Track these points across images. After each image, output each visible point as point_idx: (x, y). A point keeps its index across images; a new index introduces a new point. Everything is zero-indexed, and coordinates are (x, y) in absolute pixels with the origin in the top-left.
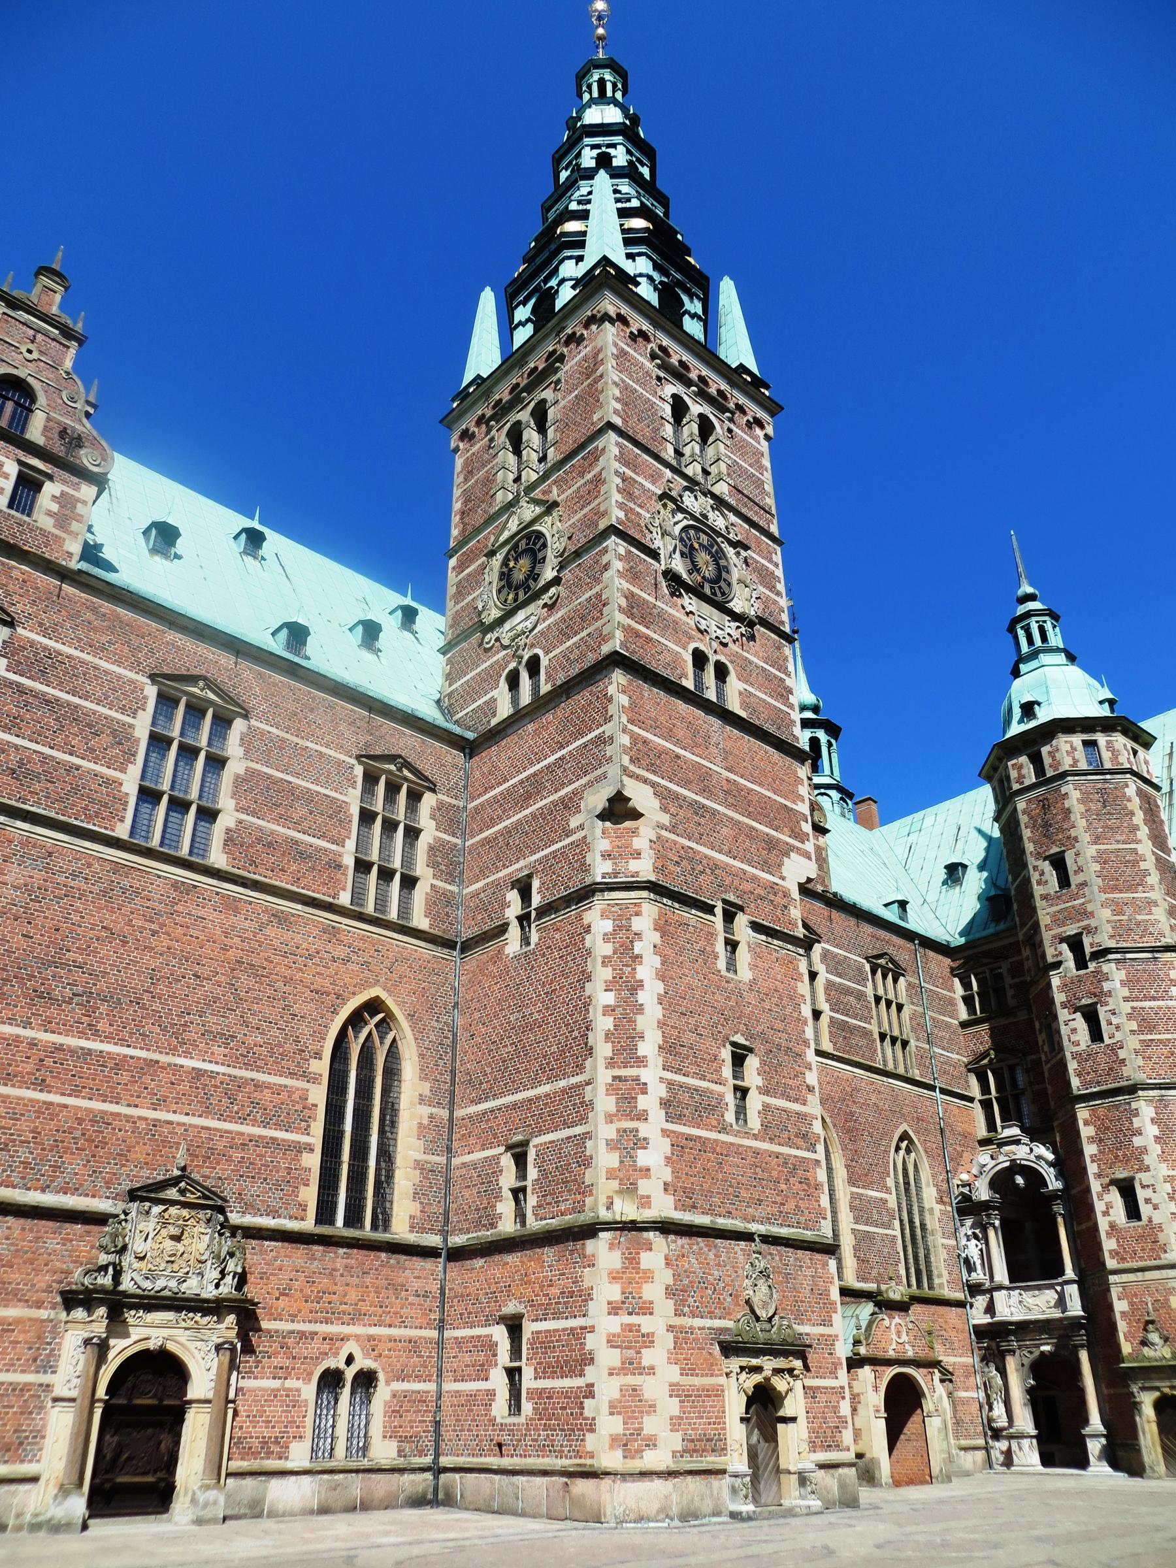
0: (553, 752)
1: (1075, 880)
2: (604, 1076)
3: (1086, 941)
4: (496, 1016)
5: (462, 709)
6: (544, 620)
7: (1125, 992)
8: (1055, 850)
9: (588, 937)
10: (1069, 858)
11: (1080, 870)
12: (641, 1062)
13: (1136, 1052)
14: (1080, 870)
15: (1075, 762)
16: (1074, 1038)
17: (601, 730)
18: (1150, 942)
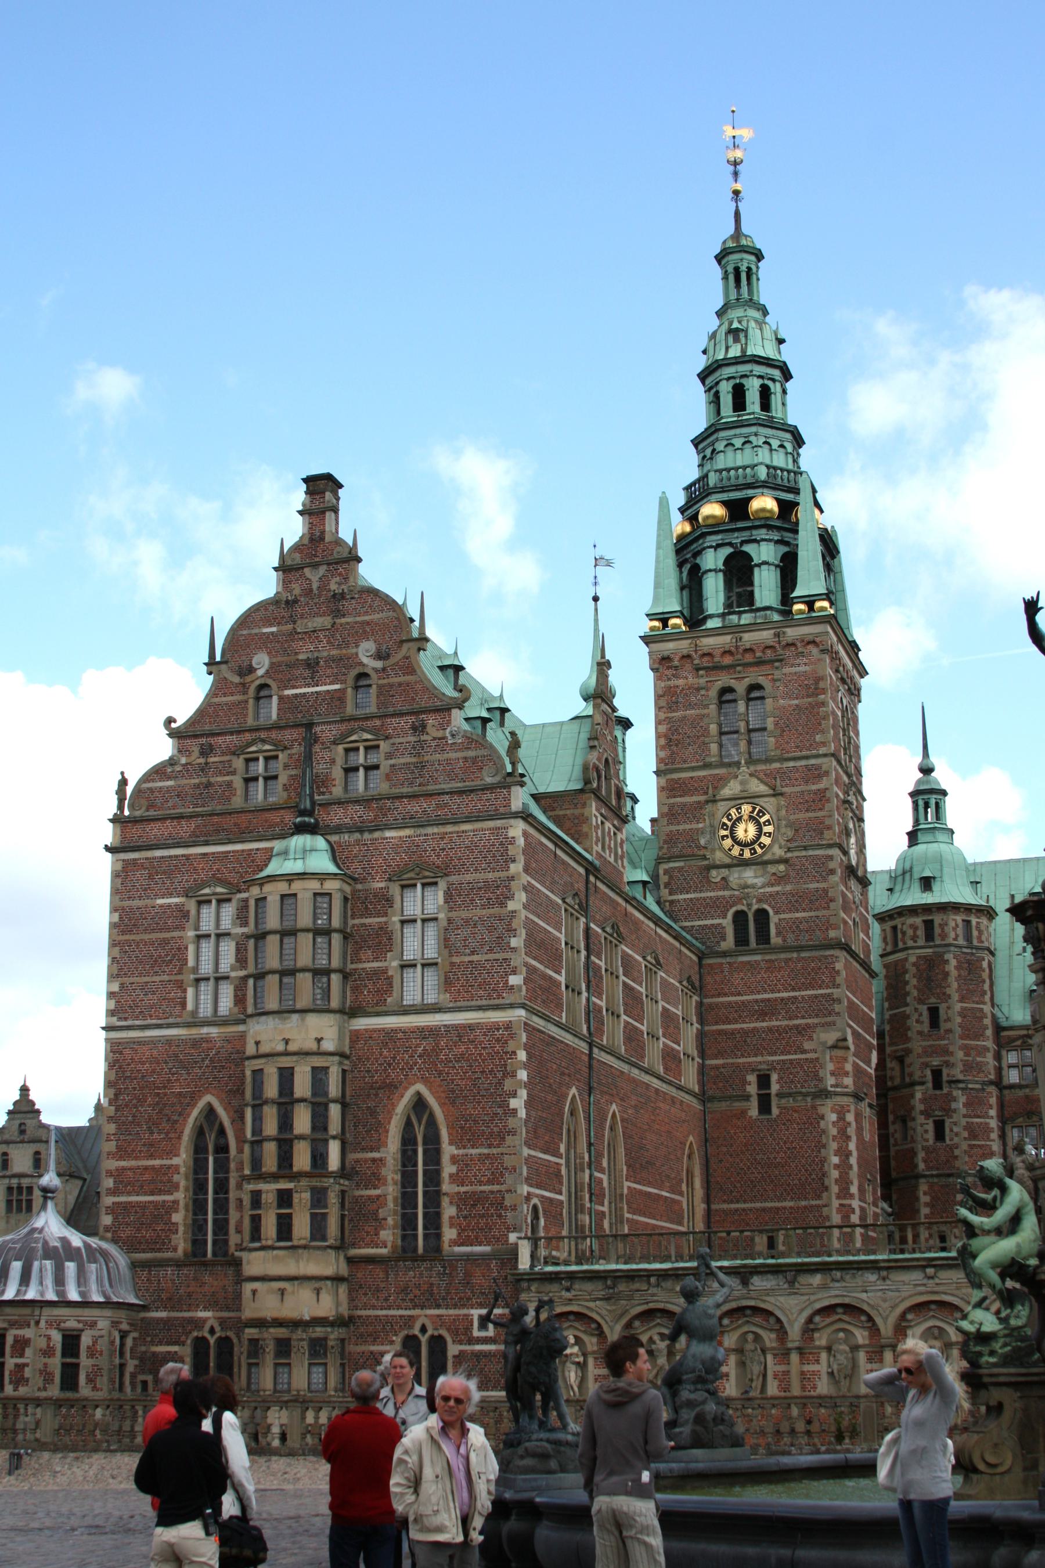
0: (786, 990)
1: (943, 1026)
2: (836, 1203)
3: (945, 1071)
4: (742, 1152)
5: (686, 919)
6: (772, 885)
7: (964, 1111)
8: (933, 1000)
9: (822, 1124)
10: (942, 1008)
11: (948, 1020)
12: (852, 1196)
13: (965, 1152)
14: (948, 1020)
15: (957, 936)
16: (926, 1136)
17: (829, 991)
18: (981, 1077)
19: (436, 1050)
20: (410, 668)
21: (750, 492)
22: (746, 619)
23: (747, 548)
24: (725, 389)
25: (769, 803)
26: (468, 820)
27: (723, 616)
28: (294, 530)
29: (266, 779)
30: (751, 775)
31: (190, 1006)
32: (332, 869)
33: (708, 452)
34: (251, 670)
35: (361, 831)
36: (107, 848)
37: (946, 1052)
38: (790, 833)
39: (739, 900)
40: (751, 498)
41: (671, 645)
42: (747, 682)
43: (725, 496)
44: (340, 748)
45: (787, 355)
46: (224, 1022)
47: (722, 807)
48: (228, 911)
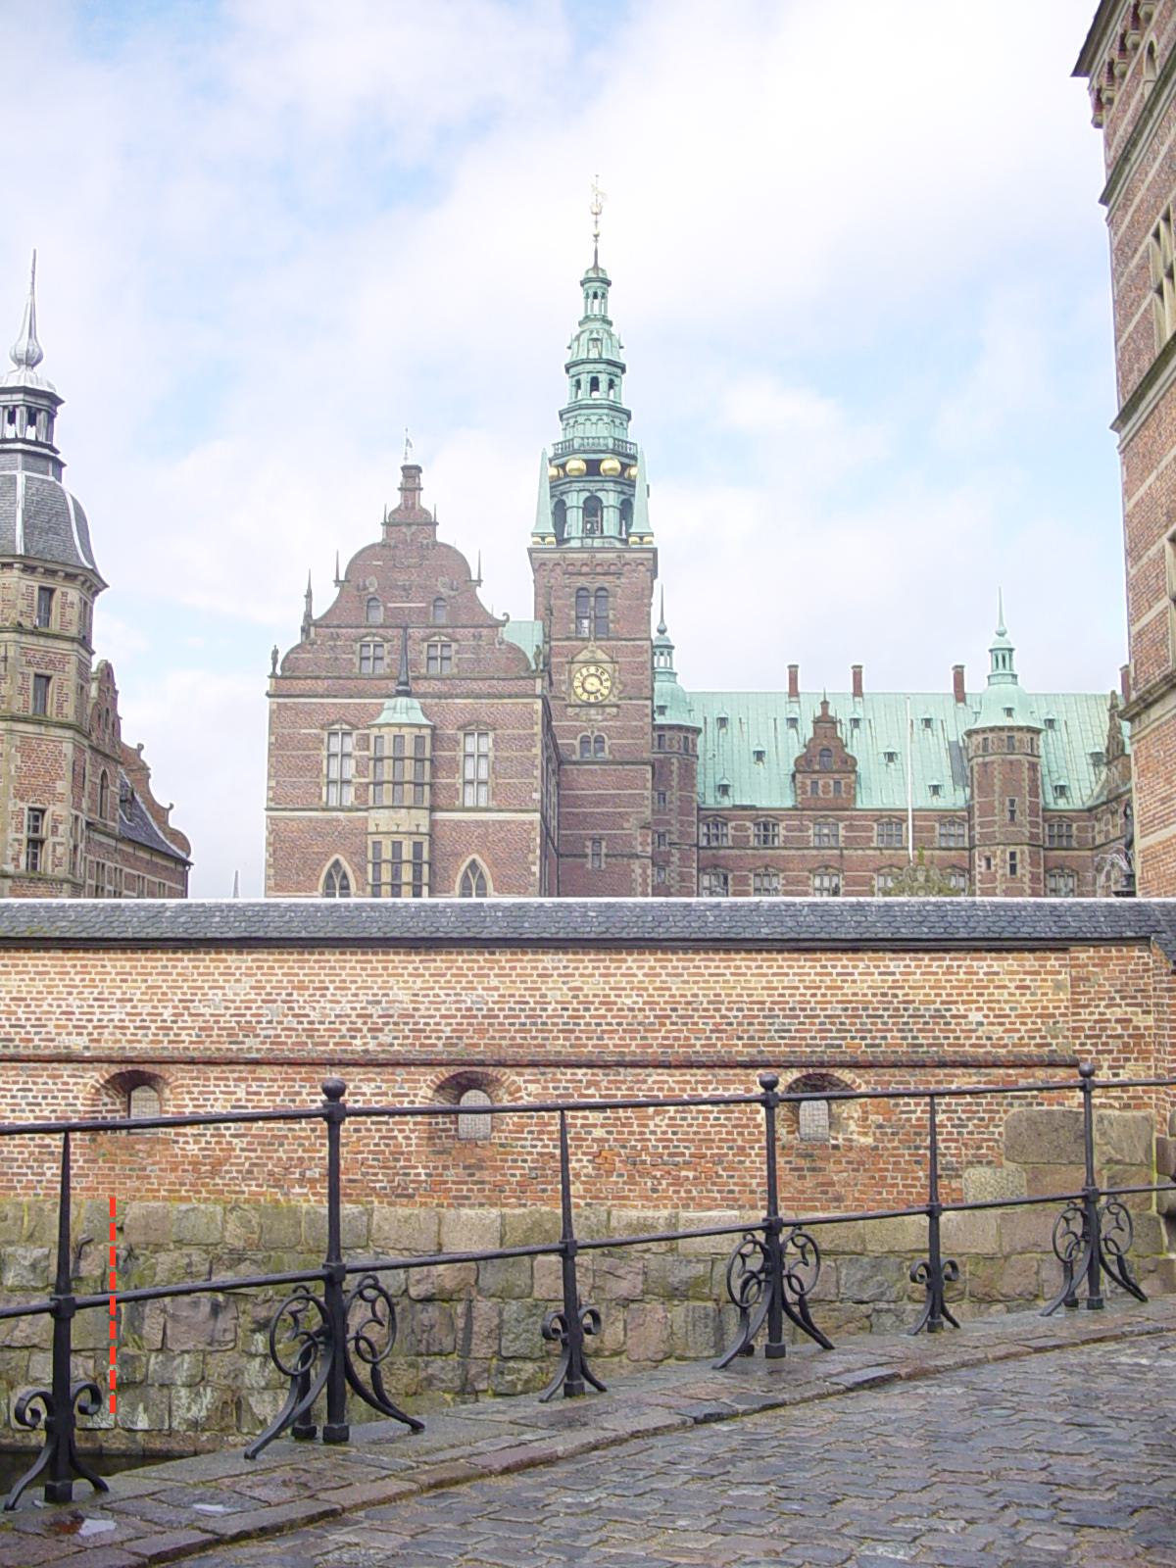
19: (486, 835)
20: (474, 598)
21: (602, 456)
22: (597, 543)
23: (600, 494)
24: (585, 379)
25: (609, 667)
26: (510, 696)
27: (582, 538)
28: (395, 500)
29: (375, 659)
30: (599, 647)
31: (324, 799)
32: (425, 722)
33: (572, 421)
34: (365, 588)
35: (440, 698)
36: (269, 695)
37: (669, 823)
38: (620, 687)
39: (586, 730)
40: (600, 461)
41: (547, 555)
42: (597, 585)
43: (585, 456)
44: (426, 644)
45: (622, 357)
46: (350, 810)
47: (576, 666)
48: (349, 744)
